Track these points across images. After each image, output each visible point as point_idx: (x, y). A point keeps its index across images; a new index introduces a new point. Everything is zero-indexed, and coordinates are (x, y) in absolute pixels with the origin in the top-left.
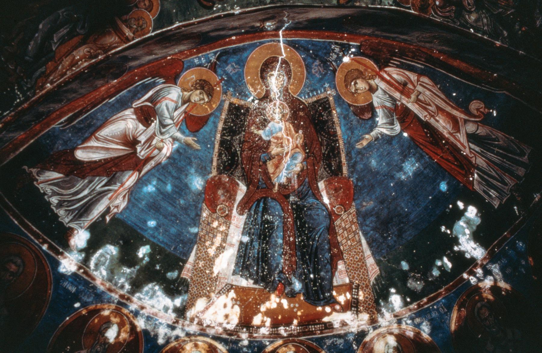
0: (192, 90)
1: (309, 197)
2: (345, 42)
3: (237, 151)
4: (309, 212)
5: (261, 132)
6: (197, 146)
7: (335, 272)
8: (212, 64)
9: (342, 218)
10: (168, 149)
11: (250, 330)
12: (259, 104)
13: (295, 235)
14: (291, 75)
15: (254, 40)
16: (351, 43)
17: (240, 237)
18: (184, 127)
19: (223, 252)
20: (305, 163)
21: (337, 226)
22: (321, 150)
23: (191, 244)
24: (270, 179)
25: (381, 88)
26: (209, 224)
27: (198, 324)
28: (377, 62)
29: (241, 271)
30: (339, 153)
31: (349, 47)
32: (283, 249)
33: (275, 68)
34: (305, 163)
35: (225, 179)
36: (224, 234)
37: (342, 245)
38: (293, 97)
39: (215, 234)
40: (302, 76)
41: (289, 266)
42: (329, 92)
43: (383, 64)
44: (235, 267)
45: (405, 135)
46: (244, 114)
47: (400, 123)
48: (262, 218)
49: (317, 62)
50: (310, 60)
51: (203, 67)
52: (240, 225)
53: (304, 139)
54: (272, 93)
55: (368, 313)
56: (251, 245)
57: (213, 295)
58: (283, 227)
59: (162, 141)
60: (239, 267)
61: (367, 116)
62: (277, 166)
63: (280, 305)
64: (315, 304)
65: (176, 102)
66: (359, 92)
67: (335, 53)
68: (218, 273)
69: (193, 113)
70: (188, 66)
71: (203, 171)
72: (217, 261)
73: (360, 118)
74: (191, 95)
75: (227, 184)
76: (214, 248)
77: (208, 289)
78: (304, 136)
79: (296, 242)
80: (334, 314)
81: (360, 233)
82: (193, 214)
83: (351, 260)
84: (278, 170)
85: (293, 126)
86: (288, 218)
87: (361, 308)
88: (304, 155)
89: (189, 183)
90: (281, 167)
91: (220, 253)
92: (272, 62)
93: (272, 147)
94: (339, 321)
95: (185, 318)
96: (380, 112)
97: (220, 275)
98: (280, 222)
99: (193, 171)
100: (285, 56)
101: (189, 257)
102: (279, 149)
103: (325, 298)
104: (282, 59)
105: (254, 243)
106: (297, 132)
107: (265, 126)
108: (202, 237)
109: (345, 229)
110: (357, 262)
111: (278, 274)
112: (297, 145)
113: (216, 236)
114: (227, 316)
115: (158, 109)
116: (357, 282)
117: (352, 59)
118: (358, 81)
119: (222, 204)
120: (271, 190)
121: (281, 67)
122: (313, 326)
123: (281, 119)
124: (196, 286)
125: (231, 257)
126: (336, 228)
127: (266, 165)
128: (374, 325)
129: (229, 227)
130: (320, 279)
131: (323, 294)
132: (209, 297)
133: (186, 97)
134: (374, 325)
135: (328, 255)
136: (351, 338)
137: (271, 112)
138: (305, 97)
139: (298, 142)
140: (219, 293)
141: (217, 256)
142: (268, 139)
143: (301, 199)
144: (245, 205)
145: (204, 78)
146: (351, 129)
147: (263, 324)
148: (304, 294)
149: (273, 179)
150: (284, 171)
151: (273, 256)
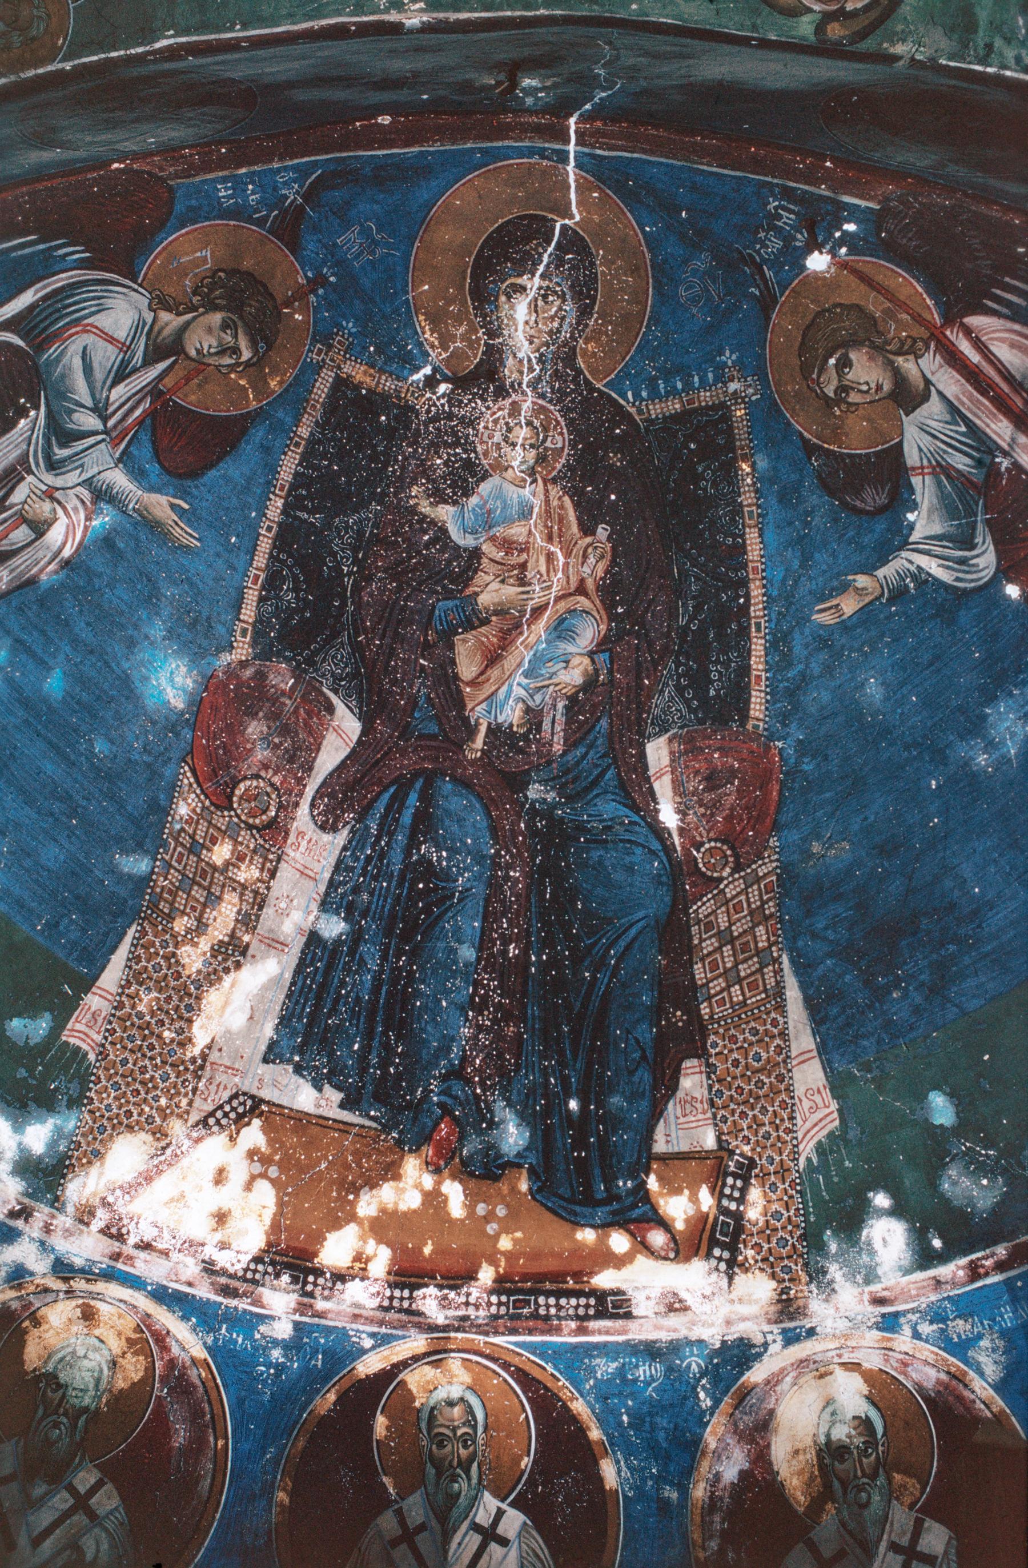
0: (194, 309)
1: (606, 792)
2: (823, 190)
3: (341, 575)
4: (596, 854)
5: (445, 513)
6: (184, 534)
7: (667, 1098)
8: (284, 212)
9: (722, 891)
10: (70, 530)
11: (305, 1283)
12: (449, 396)
13: (528, 934)
14: (593, 299)
15: (465, 139)
16: (847, 199)
17: (312, 918)
18: (144, 452)
19: (238, 966)
20: (603, 658)
21: (698, 922)
22: (673, 615)
23: (115, 916)
24: (459, 702)
25: (940, 393)
26: (195, 848)
27: (105, 1232)
28: (937, 286)
29: (301, 1050)
30: (744, 632)
31: (838, 213)
32: (477, 984)
33: (536, 264)
34: (603, 658)
35: (282, 678)
36: (249, 896)
37: (709, 998)
38: (591, 389)
39: (216, 890)
40: (635, 308)
41: (489, 1055)
42: (733, 386)
43: (961, 299)
44: (277, 1029)
45: (1013, 591)
46: (390, 433)
47: (996, 543)
48: (408, 854)
49: (702, 262)
50: (673, 248)
51: (250, 220)
52: (317, 867)
53: (613, 562)
54: (510, 362)
55: (773, 1276)
56: (352, 952)
57: (177, 1128)
58: (487, 901)
59: (50, 494)
60: (294, 1034)
61: (873, 498)
62: (492, 658)
63: (434, 1199)
64: (575, 1214)
65: (125, 348)
66: (854, 398)
67: (779, 231)
68: (209, 1047)
69: (190, 399)
70: (190, 209)
71: (197, 635)
72: (213, 998)
73: (845, 505)
74: (187, 325)
75: (288, 702)
76: (205, 944)
77: (163, 1101)
78: (614, 549)
79: (528, 964)
80: (642, 1261)
81: (785, 959)
82: (136, 803)
83: (736, 1063)
84: (494, 673)
85: (577, 505)
86: (510, 866)
87: (750, 1253)
88: (603, 627)
89: (135, 675)
90: (509, 662)
91: (227, 971)
93: (481, 578)
94: (656, 1293)
95: (57, 1203)
96: (924, 489)
97: (214, 1056)
98: (477, 878)
99: (157, 630)
100: (578, 218)
101: (103, 968)
102: (511, 591)
103: (612, 1197)
104: (564, 227)
105: (363, 948)
106: (587, 530)
107: (467, 493)
108: (161, 897)
109: (726, 938)
110: (756, 1071)
111: (444, 1078)
112: (582, 581)
113: (220, 898)
114: (221, 1218)
115: (48, 363)
116: (746, 1149)
117: (843, 265)
118: (853, 356)
119: (257, 777)
120: (459, 747)
121: (558, 261)
122: (552, 1301)
123: (532, 472)
124: (116, 1086)
125: (265, 988)
126: (694, 930)
127: (451, 647)
128: (791, 1325)
129: (273, 874)
130: (601, 1120)
131: (609, 1181)
132: (160, 1133)
133: (166, 332)
134: (791, 1325)
135: (646, 1033)
136: (694, 1363)
137: (498, 437)
138: (637, 395)
139: (587, 570)
140: (204, 1122)
141: (212, 977)
142: (468, 541)
143: (571, 799)
144: (346, 796)
145: (247, 264)
146: (804, 546)
147: (358, 1269)
148: (533, 1173)
149: (469, 707)
150: (519, 678)
151: (434, 1009)
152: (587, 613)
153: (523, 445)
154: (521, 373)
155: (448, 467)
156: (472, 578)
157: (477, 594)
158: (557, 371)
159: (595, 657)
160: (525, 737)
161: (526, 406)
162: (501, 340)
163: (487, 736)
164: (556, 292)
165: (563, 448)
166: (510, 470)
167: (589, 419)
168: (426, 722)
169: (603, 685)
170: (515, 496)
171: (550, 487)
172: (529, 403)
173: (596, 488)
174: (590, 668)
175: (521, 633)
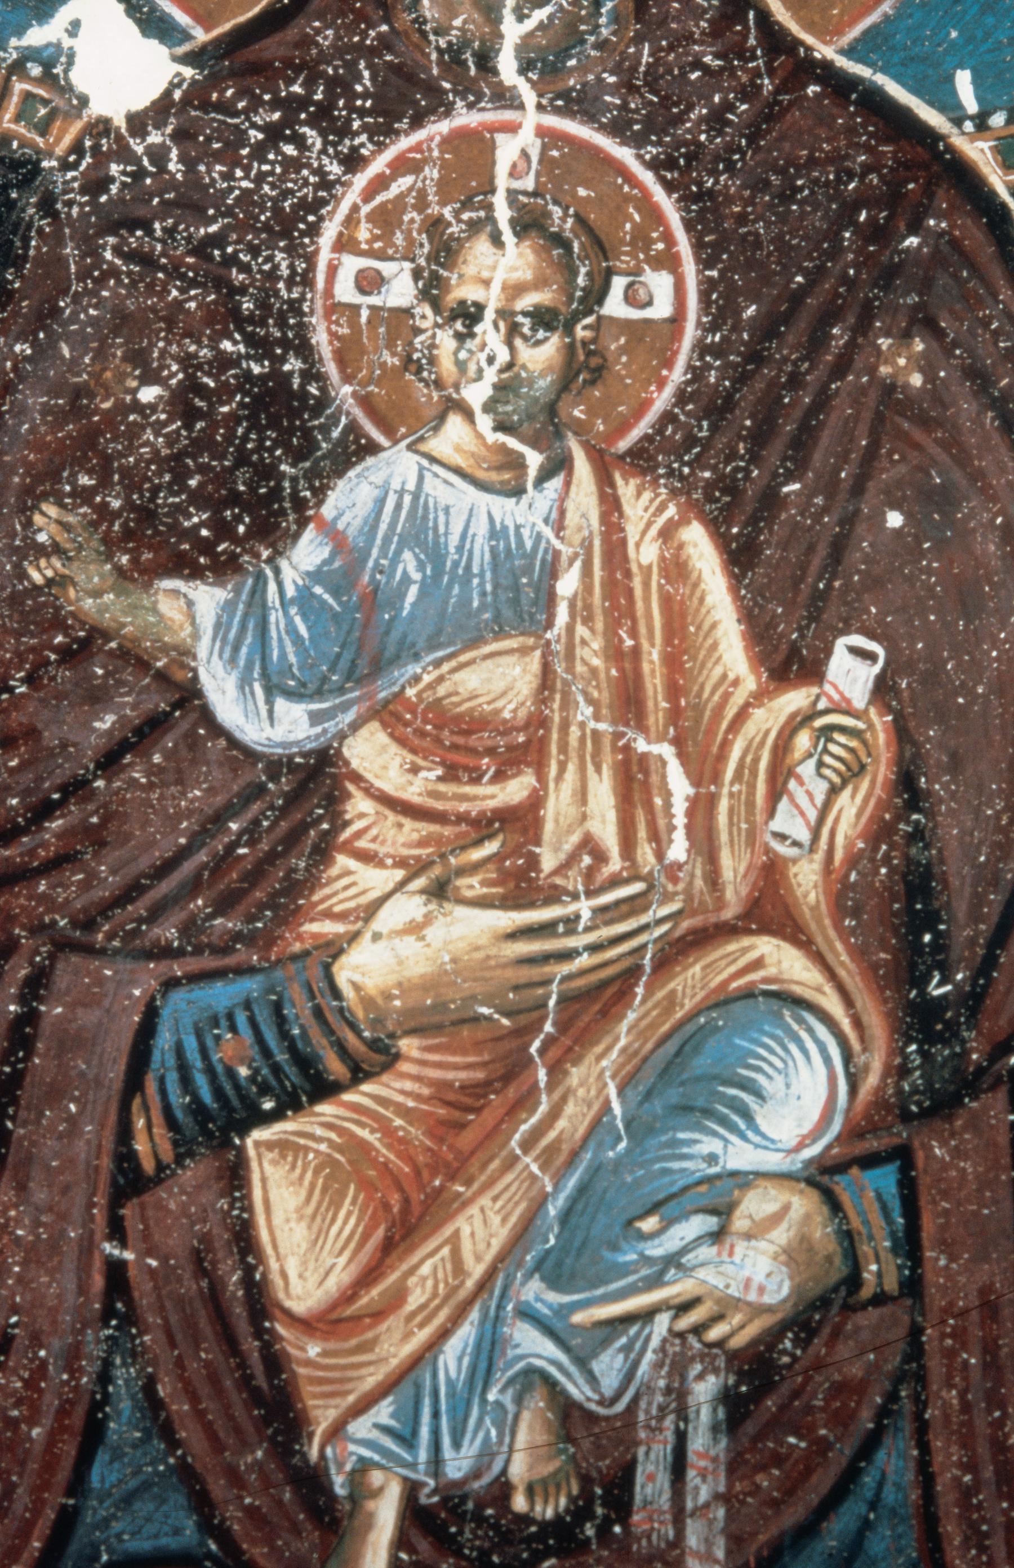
53: (908, 789)
85: (739, 558)
93: (350, 880)
102: (473, 929)
127: (235, 1176)
137: (401, 289)
149: (323, 1416)
152: (799, 1002)
153: (503, 313)
155: (190, 416)
156: (311, 882)
157: (334, 949)
159: (842, 1185)
160: (562, 1534)
161: (516, 150)
163: (401, 1541)
165: (677, 320)
166: (455, 422)
167: (787, 194)
168: (143, 1507)
169: (880, 1299)
170: (480, 528)
171: (626, 488)
172: (527, 138)
173: (830, 487)
174: (823, 1233)
175: (527, 1100)
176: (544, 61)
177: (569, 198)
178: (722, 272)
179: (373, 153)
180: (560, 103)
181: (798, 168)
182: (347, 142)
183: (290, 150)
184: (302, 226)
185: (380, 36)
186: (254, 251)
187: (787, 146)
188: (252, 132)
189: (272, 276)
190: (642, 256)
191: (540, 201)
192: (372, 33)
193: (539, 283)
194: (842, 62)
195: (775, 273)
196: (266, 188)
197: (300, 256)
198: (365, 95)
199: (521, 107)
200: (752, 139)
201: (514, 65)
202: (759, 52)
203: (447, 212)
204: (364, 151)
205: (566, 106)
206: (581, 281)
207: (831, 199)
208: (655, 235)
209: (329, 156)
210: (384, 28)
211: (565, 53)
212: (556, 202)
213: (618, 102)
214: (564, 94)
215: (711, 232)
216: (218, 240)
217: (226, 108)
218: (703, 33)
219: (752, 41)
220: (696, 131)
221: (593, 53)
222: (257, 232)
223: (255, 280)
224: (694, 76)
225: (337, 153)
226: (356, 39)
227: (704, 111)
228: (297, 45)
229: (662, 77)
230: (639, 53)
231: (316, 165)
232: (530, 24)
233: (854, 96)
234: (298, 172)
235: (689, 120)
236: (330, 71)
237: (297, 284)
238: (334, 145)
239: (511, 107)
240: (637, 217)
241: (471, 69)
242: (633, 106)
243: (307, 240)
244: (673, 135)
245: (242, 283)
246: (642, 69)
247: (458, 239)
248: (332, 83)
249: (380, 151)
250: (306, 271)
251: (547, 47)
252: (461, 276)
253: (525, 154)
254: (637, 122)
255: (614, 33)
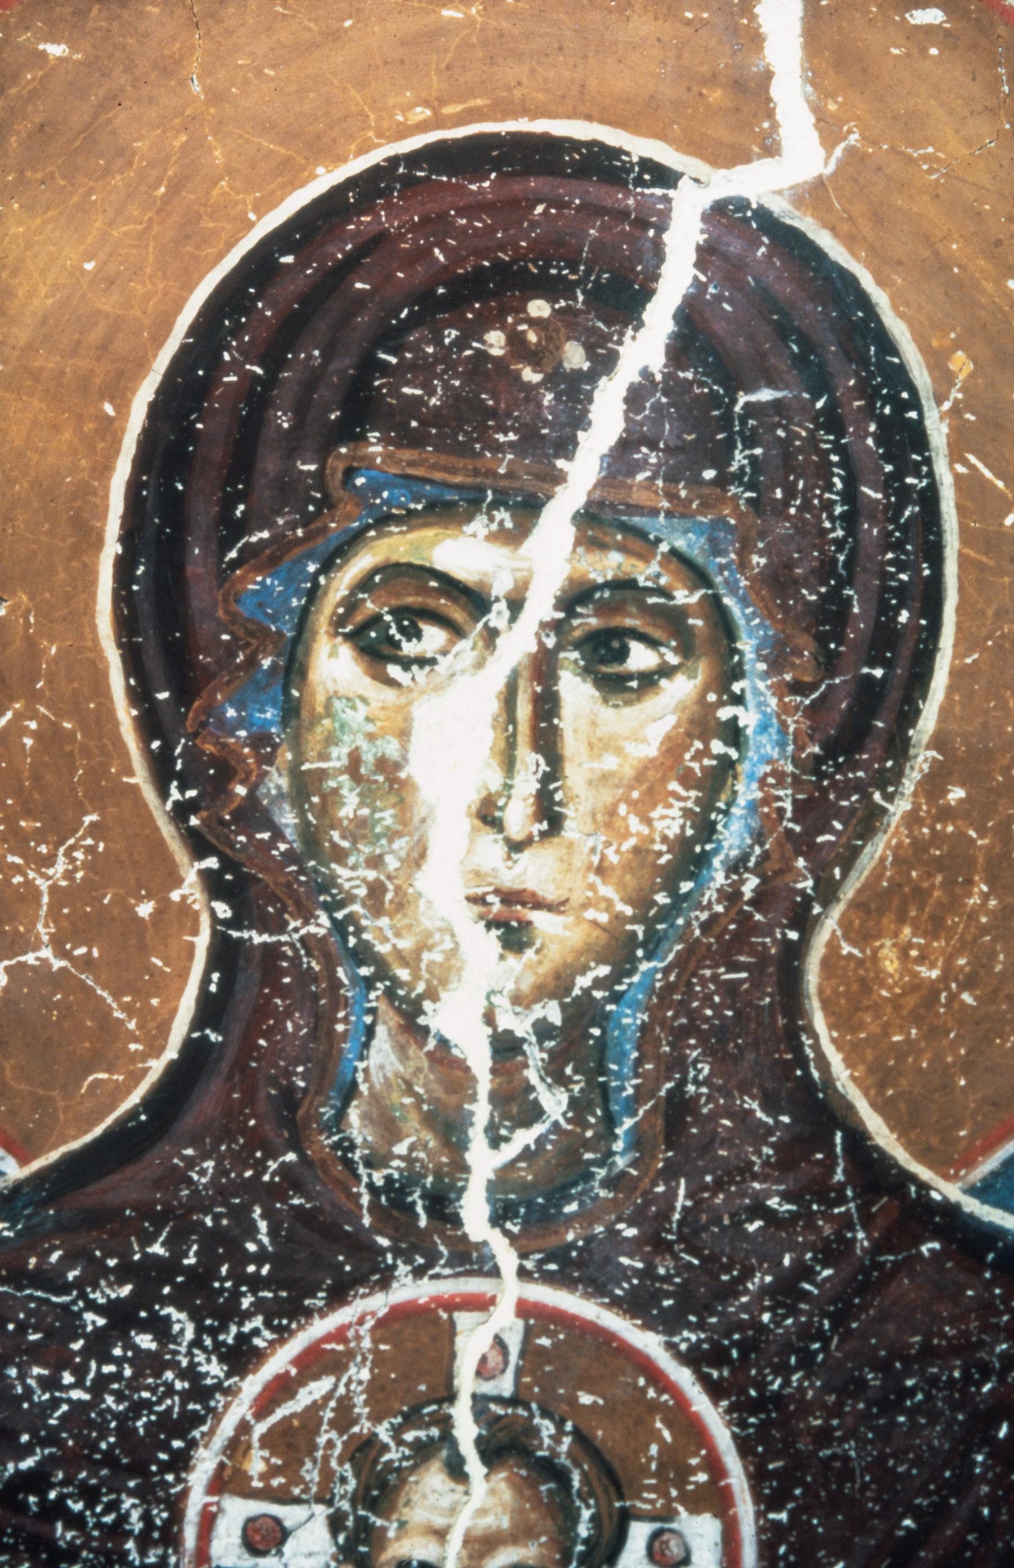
54: (382, 1059)
92: (493, 286)
121: (688, 430)
154: (451, 1130)
158: (678, 1110)
162: (321, 925)
164: (674, 619)
167: (892, 1399)
172: (505, 1321)
176: (529, 1205)
177: (564, 1407)
178: (792, 1514)
179: (272, 1343)
180: (553, 1267)
181: (907, 1361)
182: (234, 1329)
183: (145, 1341)
184: (163, 1456)
185: (284, 1169)
186: (90, 1495)
187: (891, 1328)
188: (89, 1317)
189: (118, 1531)
190: (674, 1493)
191: (521, 1412)
192: (273, 1165)
193: (520, 1534)
194: (972, 1206)
195: (872, 1514)
196: (110, 1400)
197: (159, 1501)
198: (260, 1258)
199: (495, 1272)
200: (839, 1320)
201: (485, 1210)
202: (849, 1193)
203: (383, 1433)
204: (258, 1342)
205: (561, 1271)
206: (583, 1530)
207: (956, 1407)
208: (694, 1461)
209: (204, 1349)
210: (291, 1157)
211: (560, 1194)
212: (545, 1414)
213: (640, 1265)
214: (559, 1253)
215: (776, 1456)
216: (36, 1480)
217: (50, 1280)
218: (766, 1163)
219: (839, 1176)
220: (755, 1307)
221: (603, 1193)
222: (94, 1467)
223: (90, 1538)
224: (753, 1227)
225: (218, 1345)
226: (248, 1174)
227: (768, 1279)
228: (158, 1184)
229: (705, 1228)
230: (671, 1195)
231: (185, 1363)
232: (509, 1151)
233: (991, 1256)
234: (158, 1375)
235: (746, 1292)
236: (209, 1222)
237: (156, 1543)
238: (213, 1332)
239: (480, 1273)
240: (667, 1435)
241: (421, 1220)
242: (662, 1271)
243: (170, 1478)
244: (722, 1314)
245: (71, 1543)
246: (677, 1216)
247: (399, 1470)
248: (210, 1239)
249: (282, 1341)
250: (168, 1523)
251: (534, 1185)
252: (402, 1525)
253: (500, 1343)
254: (668, 1295)
255: (634, 1164)
